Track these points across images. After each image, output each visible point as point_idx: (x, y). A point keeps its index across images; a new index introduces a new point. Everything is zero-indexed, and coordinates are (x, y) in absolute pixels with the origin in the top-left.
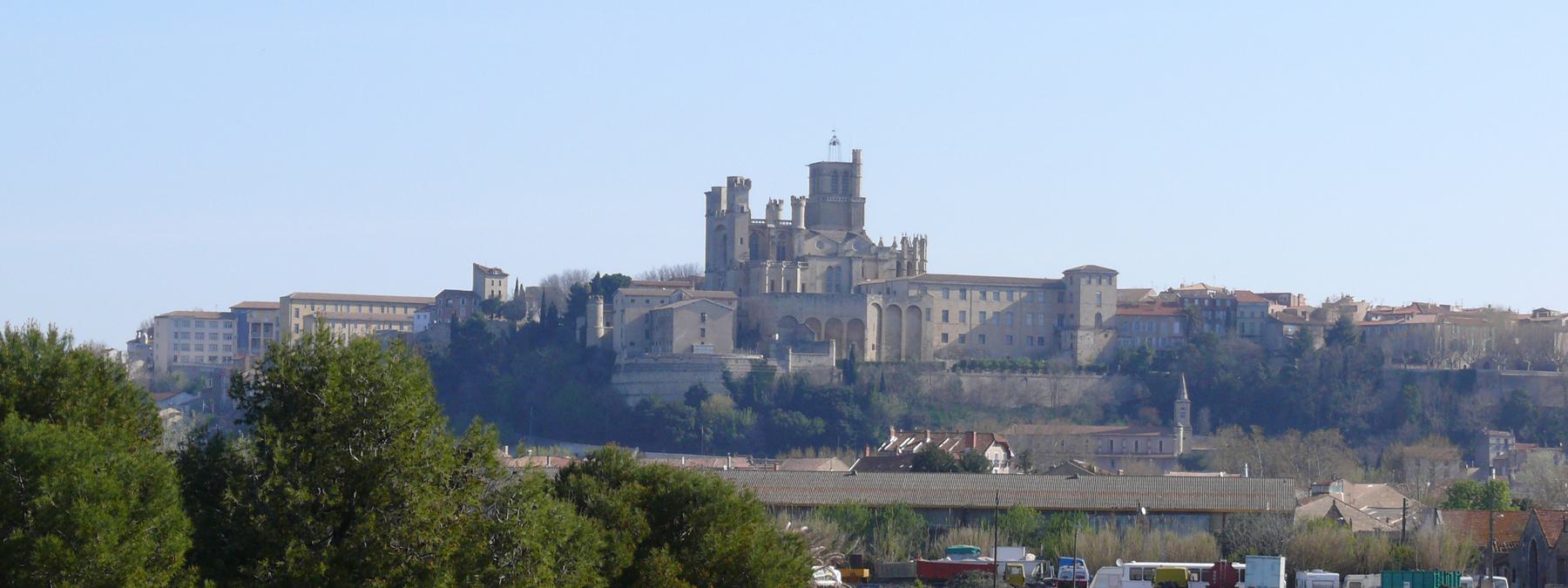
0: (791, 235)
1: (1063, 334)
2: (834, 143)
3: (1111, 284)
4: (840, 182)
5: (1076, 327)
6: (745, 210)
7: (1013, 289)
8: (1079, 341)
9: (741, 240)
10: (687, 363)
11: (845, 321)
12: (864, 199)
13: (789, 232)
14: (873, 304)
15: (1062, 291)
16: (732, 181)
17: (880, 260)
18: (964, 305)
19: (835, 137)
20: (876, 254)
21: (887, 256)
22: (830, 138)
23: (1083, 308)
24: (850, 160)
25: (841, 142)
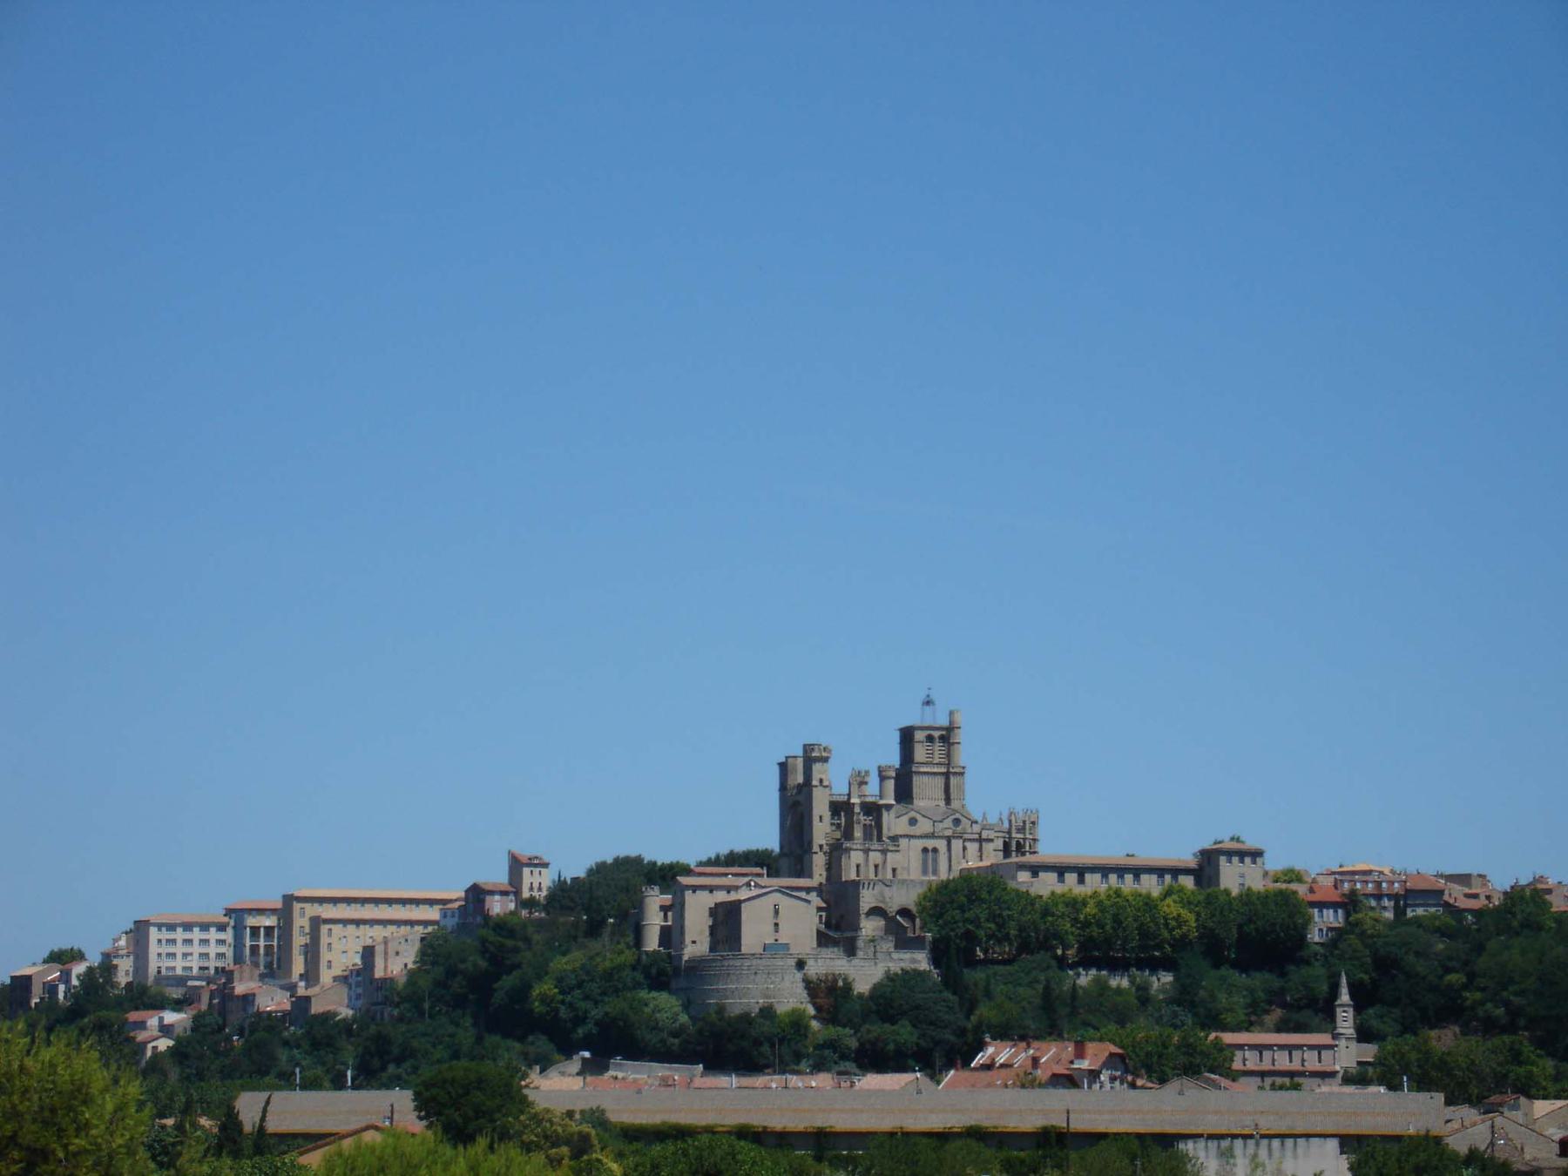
2: (928, 703)
3: (1254, 862)
4: (938, 745)
6: (825, 783)
9: (821, 817)
13: (873, 809)
16: (808, 749)
17: (984, 840)
19: (928, 696)
20: (980, 834)
21: (992, 835)
22: (922, 696)
24: (943, 721)
25: (937, 703)
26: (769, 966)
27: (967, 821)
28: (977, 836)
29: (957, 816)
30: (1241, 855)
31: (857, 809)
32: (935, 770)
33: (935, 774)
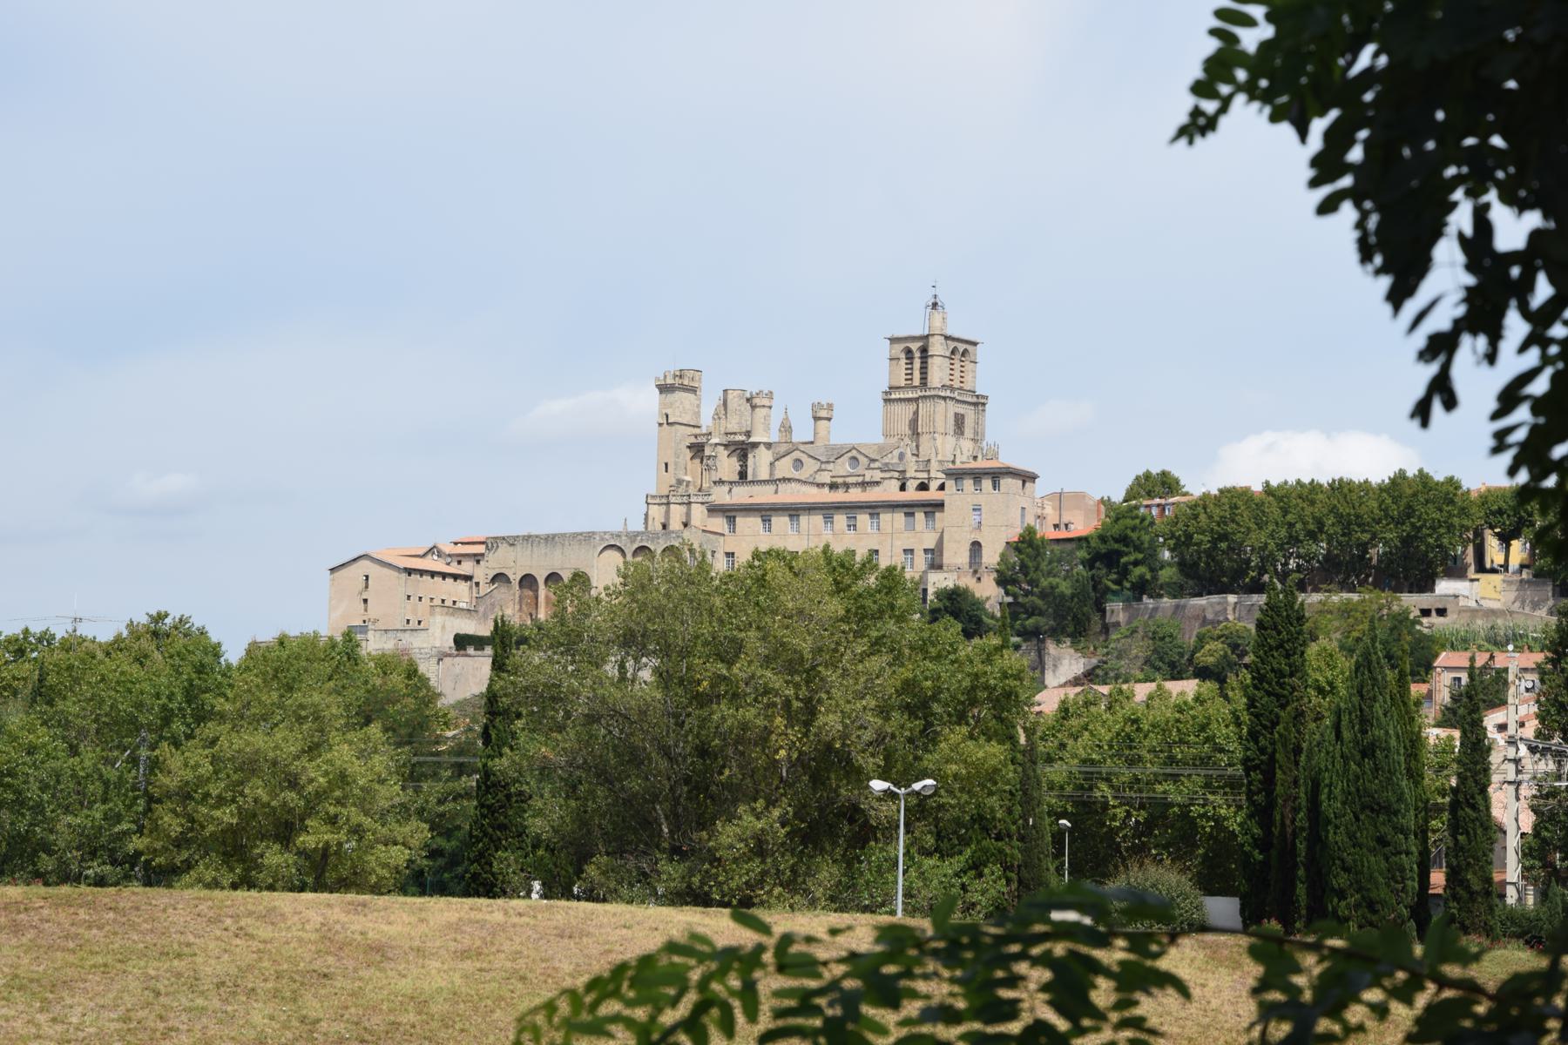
4: (917, 364)
9: (666, 465)
17: (867, 483)
27: (866, 459)
28: (860, 479)
29: (854, 453)
33: (909, 400)
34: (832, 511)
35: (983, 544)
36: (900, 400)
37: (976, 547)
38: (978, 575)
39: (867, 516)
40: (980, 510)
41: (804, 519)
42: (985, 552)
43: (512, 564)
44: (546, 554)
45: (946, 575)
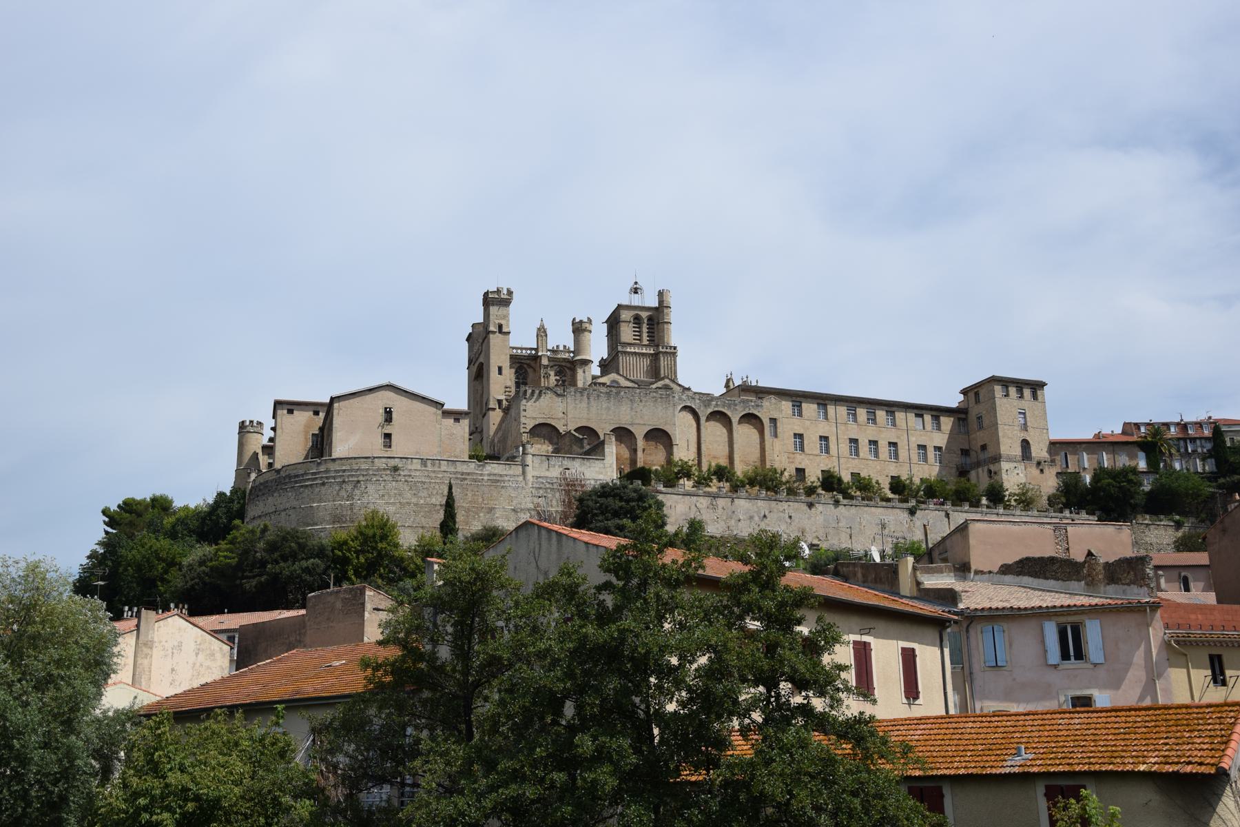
0: (574, 371)
1: (973, 474)
2: (636, 292)
3: (1035, 397)
4: (645, 329)
5: (997, 459)
6: (505, 330)
7: (894, 409)
8: (1004, 476)
9: (500, 369)
10: (327, 471)
11: (639, 433)
12: (675, 348)
14: (685, 408)
15: (963, 416)
18: (824, 428)
19: (636, 283)
22: (631, 284)
23: (1002, 431)
26: (344, 471)
27: (678, 388)
30: (1020, 385)
31: (545, 362)
32: (644, 351)
33: (643, 355)
34: (854, 405)
35: (1031, 442)
36: (635, 353)
37: (1025, 445)
38: (1041, 467)
39: (884, 413)
40: (1024, 414)
41: (831, 409)
42: (1033, 449)
43: (561, 415)
44: (608, 409)
45: (1015, 464)
